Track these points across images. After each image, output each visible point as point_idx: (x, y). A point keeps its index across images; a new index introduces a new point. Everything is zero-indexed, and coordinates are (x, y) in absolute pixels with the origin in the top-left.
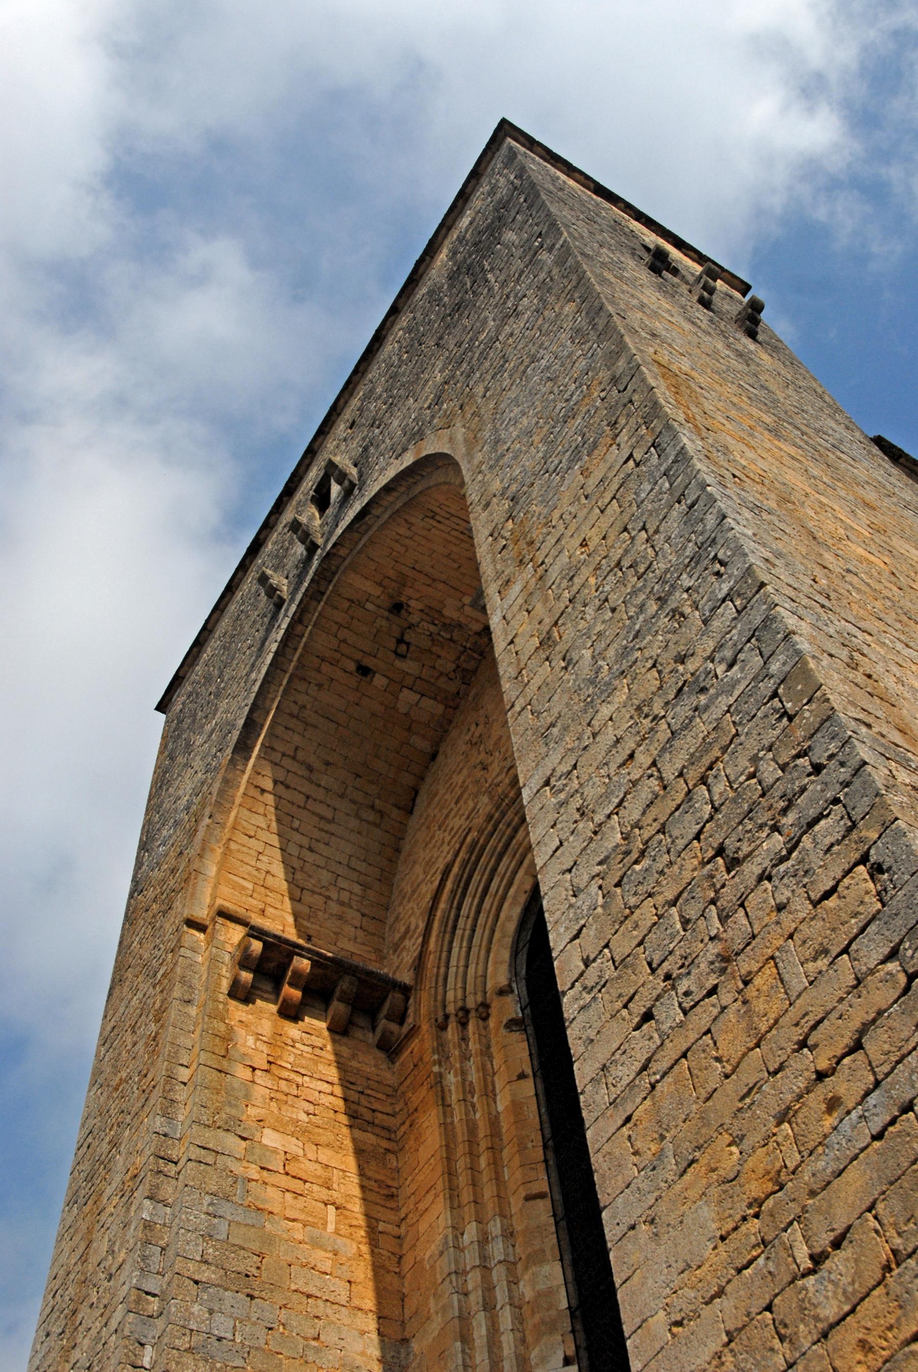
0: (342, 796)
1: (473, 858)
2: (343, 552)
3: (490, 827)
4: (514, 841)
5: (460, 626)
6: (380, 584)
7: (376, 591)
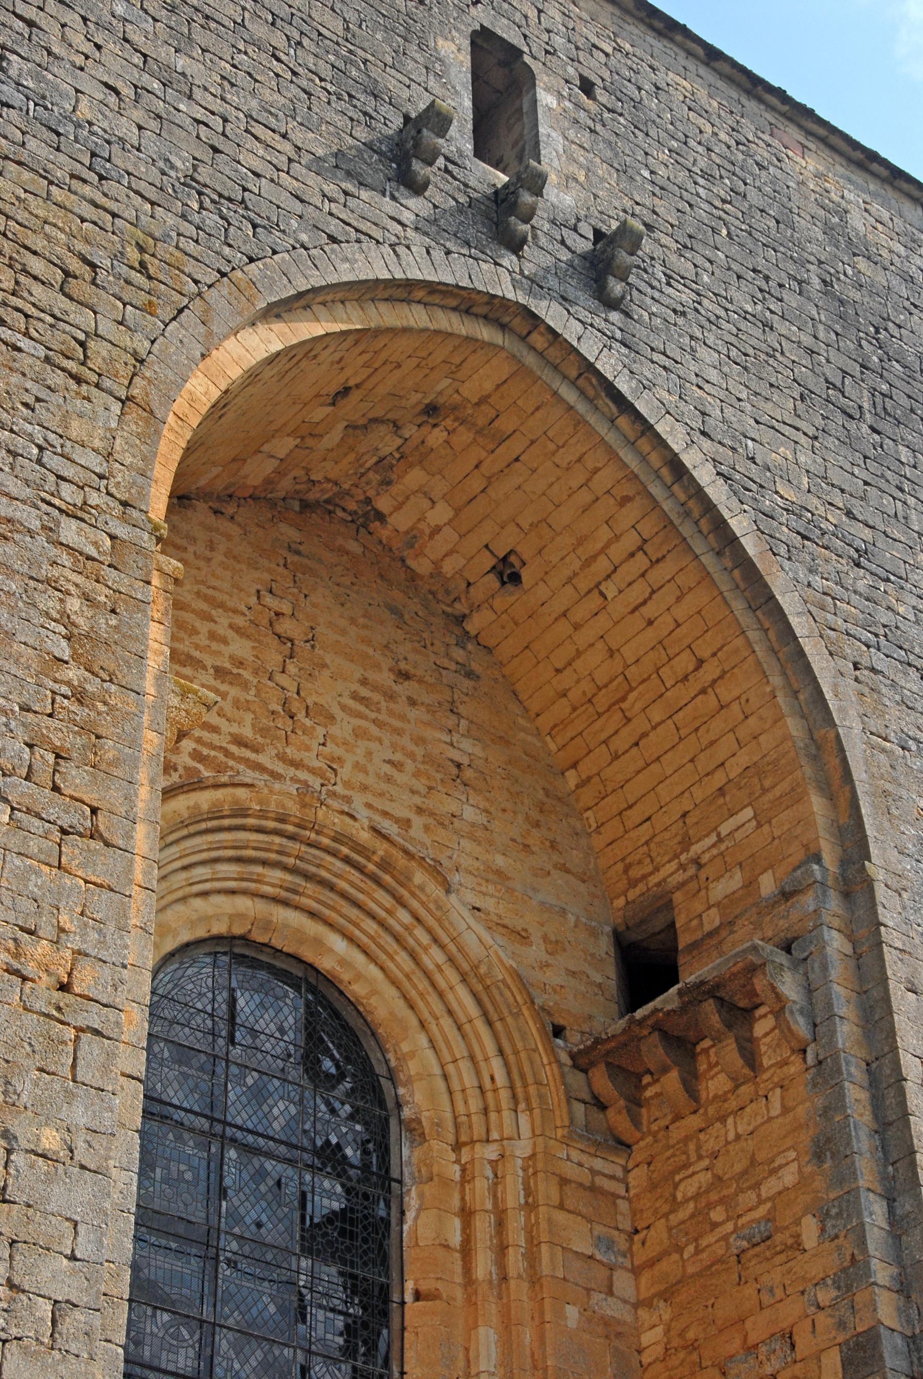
1: (226, 822)
2: (538, 340)
3: (271, 824)
4: (259, 869)
7: (470, 391)
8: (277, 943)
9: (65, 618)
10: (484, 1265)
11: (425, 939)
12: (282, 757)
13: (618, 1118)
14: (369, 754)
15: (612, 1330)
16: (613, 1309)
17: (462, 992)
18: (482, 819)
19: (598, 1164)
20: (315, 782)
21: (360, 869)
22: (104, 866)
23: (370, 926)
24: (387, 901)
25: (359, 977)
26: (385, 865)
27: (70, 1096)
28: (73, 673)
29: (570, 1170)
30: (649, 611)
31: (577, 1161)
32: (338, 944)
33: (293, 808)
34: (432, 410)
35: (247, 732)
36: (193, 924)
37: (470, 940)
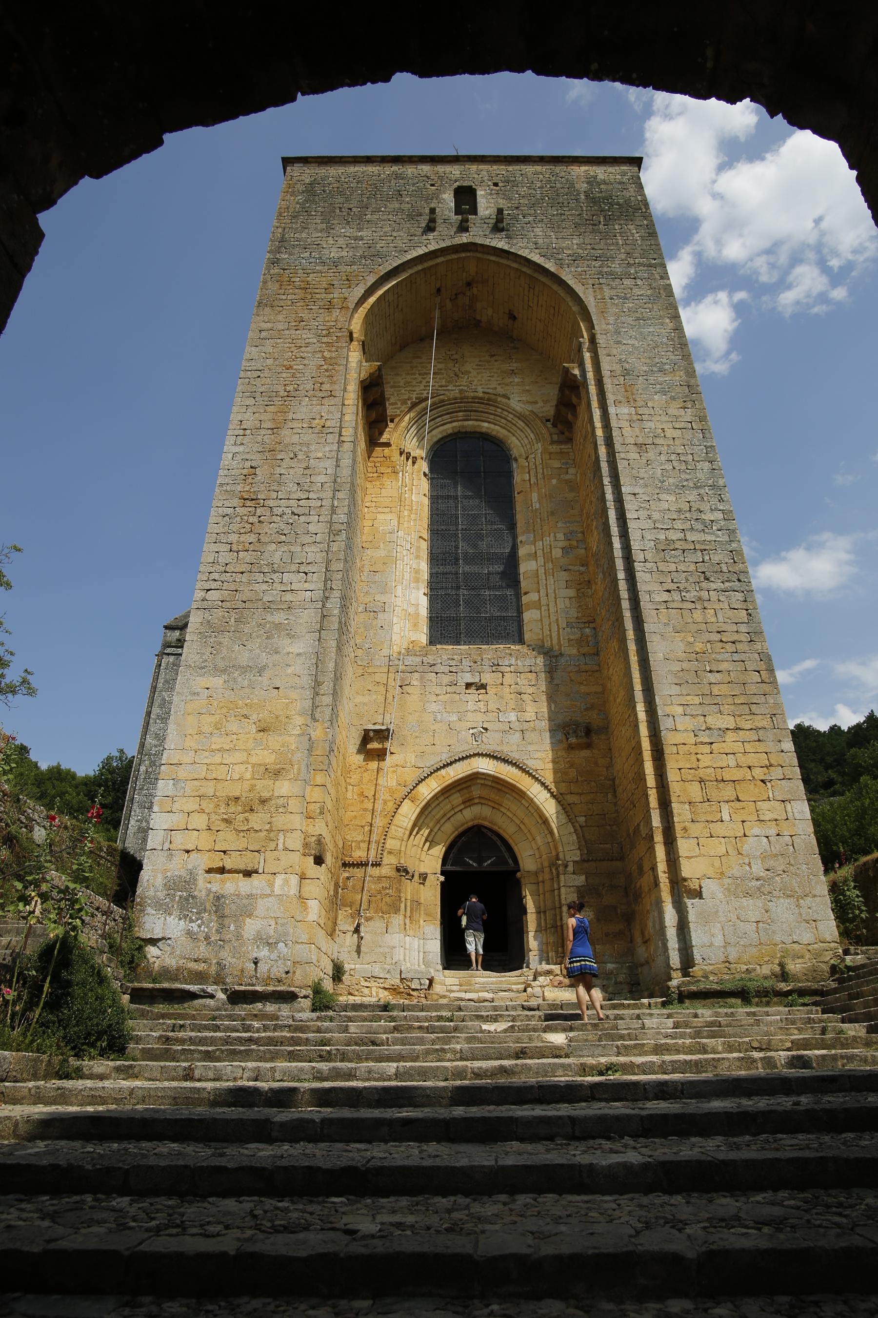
0: (395, 325)
5: (475, 311)
6: (477, 273)
8: (468, 430)
9: (323, 357)
10: (533, 480)
11: (506, 413)
12: (455, 386)
13: (567, 433)
14: (482, 377)
15: (567, 482)
16: (568, 477)
17: (520, 422)
18: (520, 380)
19: (563, 447)
20: (466, 388)
21: (483, 403)
22: (332, 401)
23: (492, 417)
24: (493, 408)
25: (493, 430)
26: (489, 400)
27: (324, 446)
28: (325, 367)
29: (552, 450)
30: (540, 303)
31: (555, 448)
32: (486, 425)
33: (458, 395)
34: (469, 284)
35: (444, 383)
36: (441, 432)
37: (518, 409)
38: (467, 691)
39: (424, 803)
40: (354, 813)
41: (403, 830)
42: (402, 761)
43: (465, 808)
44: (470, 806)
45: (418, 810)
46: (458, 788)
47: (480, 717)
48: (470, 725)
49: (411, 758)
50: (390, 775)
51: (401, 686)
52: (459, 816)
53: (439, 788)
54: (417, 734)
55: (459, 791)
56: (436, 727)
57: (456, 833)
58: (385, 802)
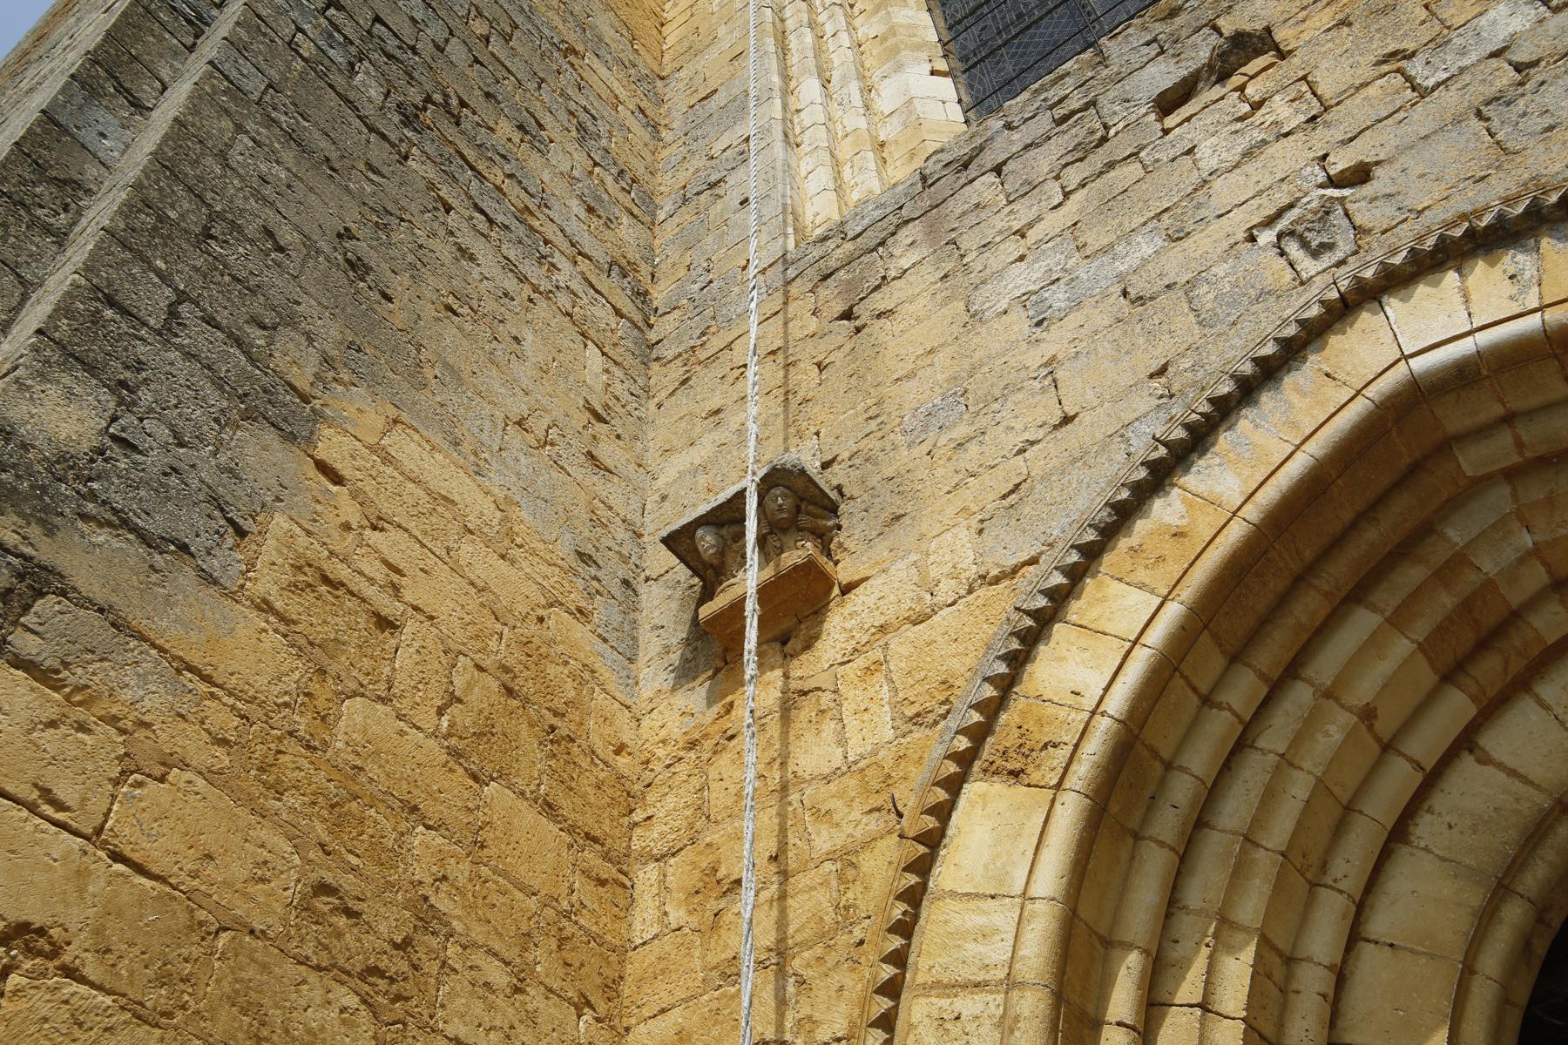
38: (1170, 121)
39: (1095, 747)
40: (676, 1016)
41: (992, 1003)
42: (913, 600)
43: (1491, 709)
44: (1521, 685)
45: (1069, 812)
46: (1339, 571)
47: (1291, 157)
48: (1241, 220)
49: (956, 550)
50: (853, 697)
51: (847, 315)
52: (1472, 789)
53: (1174, 611)
54: (961, 431)
55: (1357, 595)
56: (1055, 341)
57: (1514, 914)
58: (846, 859)
